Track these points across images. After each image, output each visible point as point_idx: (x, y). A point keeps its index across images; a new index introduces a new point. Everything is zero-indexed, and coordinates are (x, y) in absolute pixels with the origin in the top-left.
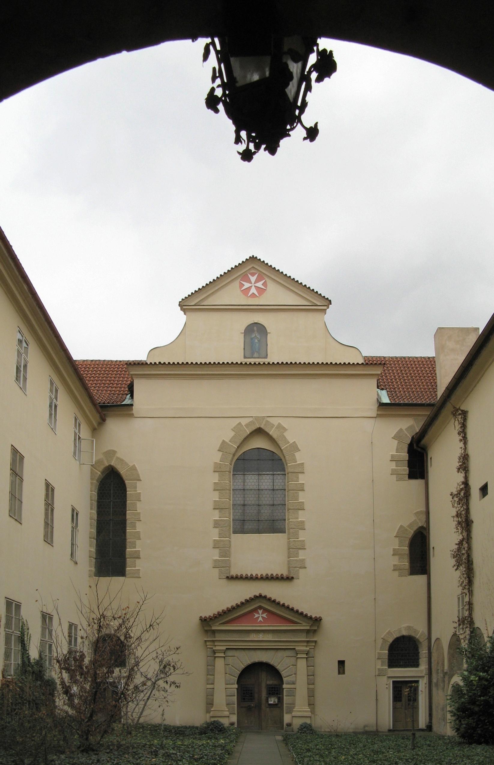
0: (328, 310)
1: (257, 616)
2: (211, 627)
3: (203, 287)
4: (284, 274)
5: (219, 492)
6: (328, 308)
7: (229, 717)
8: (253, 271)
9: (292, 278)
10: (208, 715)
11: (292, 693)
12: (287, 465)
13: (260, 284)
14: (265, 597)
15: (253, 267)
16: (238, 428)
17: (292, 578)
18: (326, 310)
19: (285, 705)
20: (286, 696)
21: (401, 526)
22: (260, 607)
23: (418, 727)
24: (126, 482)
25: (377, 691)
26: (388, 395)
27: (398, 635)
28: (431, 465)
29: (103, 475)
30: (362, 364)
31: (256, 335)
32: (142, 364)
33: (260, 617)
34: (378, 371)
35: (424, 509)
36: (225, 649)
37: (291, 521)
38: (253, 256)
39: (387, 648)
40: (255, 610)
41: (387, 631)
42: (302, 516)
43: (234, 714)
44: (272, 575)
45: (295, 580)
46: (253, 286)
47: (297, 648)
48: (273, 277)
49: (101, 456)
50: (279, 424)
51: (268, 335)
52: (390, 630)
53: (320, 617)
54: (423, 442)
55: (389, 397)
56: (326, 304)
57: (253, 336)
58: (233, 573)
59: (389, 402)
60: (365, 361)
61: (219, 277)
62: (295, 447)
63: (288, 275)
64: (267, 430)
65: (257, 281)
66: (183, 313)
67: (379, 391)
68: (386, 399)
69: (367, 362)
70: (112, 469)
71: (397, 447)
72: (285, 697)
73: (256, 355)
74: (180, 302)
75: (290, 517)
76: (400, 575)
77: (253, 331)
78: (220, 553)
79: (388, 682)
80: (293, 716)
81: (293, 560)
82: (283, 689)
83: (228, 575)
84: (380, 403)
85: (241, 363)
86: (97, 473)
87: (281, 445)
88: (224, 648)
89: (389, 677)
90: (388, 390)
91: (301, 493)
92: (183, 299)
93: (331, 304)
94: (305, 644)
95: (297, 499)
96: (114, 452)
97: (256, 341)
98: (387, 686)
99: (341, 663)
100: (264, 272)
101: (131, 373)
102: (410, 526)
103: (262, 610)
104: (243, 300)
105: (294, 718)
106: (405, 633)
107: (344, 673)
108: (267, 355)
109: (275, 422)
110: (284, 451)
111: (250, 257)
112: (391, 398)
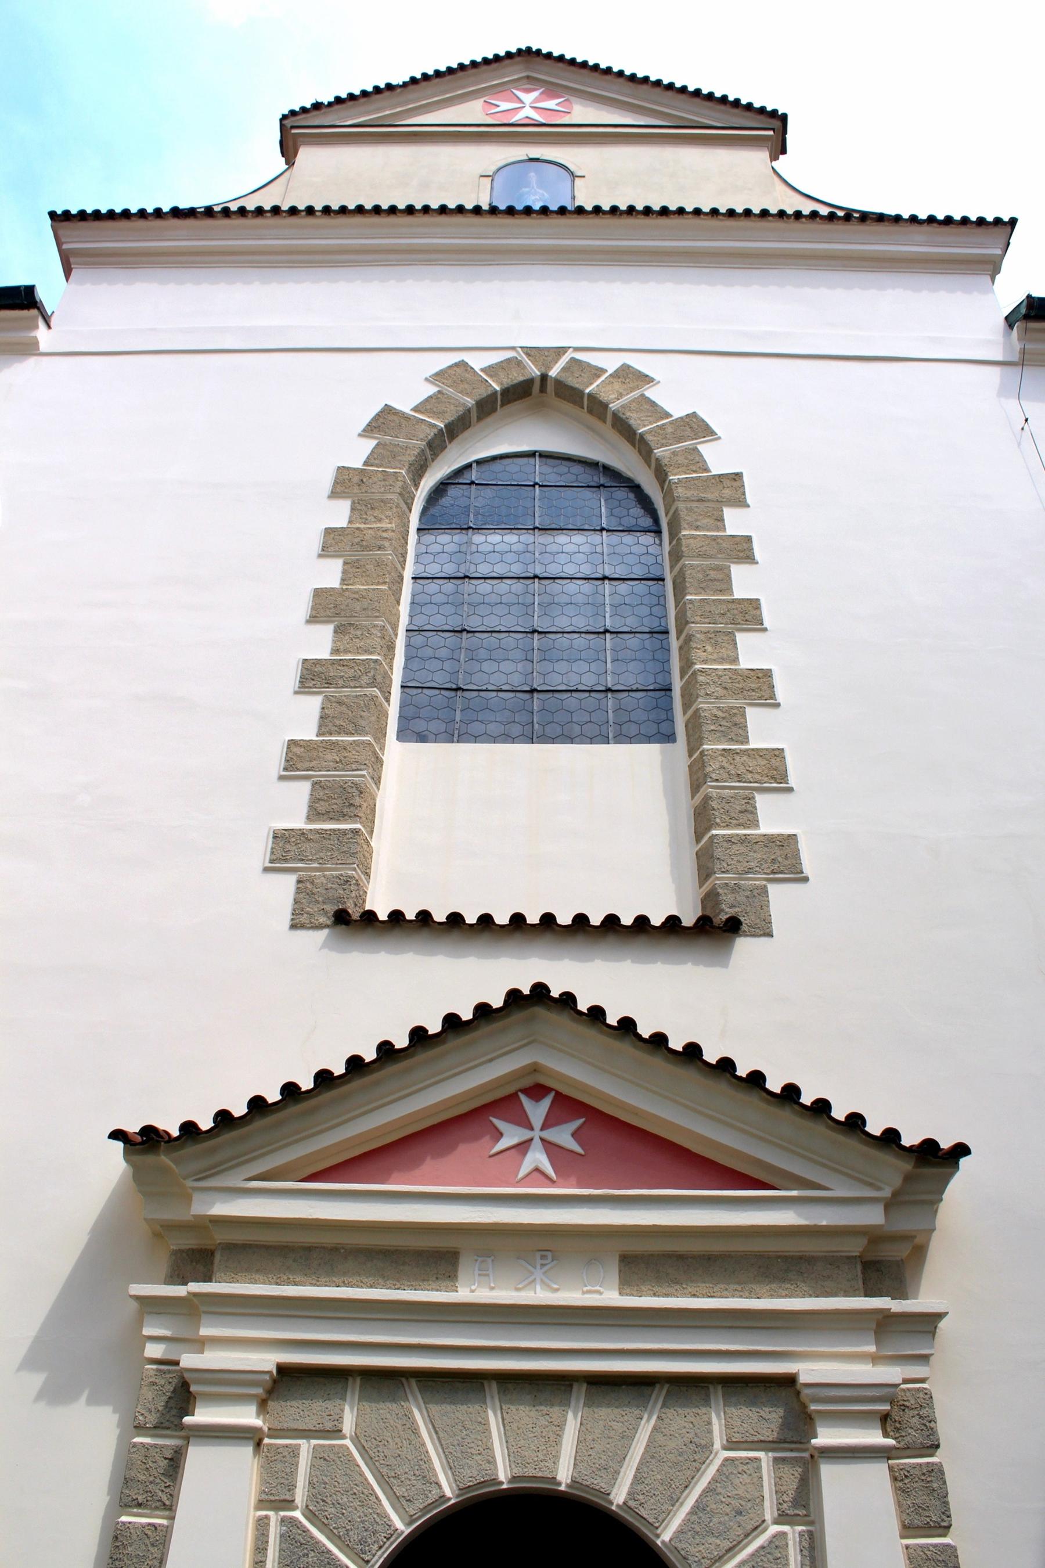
1: (512, 1135)
2: (188, 1199)
5: (345, 563)
17: (733, 927)
22: (537, 1091)
33: (537, 1143)
37: (702, 671)
81: (729, 840)
88: (267, 1361)
103: (546, 1103)
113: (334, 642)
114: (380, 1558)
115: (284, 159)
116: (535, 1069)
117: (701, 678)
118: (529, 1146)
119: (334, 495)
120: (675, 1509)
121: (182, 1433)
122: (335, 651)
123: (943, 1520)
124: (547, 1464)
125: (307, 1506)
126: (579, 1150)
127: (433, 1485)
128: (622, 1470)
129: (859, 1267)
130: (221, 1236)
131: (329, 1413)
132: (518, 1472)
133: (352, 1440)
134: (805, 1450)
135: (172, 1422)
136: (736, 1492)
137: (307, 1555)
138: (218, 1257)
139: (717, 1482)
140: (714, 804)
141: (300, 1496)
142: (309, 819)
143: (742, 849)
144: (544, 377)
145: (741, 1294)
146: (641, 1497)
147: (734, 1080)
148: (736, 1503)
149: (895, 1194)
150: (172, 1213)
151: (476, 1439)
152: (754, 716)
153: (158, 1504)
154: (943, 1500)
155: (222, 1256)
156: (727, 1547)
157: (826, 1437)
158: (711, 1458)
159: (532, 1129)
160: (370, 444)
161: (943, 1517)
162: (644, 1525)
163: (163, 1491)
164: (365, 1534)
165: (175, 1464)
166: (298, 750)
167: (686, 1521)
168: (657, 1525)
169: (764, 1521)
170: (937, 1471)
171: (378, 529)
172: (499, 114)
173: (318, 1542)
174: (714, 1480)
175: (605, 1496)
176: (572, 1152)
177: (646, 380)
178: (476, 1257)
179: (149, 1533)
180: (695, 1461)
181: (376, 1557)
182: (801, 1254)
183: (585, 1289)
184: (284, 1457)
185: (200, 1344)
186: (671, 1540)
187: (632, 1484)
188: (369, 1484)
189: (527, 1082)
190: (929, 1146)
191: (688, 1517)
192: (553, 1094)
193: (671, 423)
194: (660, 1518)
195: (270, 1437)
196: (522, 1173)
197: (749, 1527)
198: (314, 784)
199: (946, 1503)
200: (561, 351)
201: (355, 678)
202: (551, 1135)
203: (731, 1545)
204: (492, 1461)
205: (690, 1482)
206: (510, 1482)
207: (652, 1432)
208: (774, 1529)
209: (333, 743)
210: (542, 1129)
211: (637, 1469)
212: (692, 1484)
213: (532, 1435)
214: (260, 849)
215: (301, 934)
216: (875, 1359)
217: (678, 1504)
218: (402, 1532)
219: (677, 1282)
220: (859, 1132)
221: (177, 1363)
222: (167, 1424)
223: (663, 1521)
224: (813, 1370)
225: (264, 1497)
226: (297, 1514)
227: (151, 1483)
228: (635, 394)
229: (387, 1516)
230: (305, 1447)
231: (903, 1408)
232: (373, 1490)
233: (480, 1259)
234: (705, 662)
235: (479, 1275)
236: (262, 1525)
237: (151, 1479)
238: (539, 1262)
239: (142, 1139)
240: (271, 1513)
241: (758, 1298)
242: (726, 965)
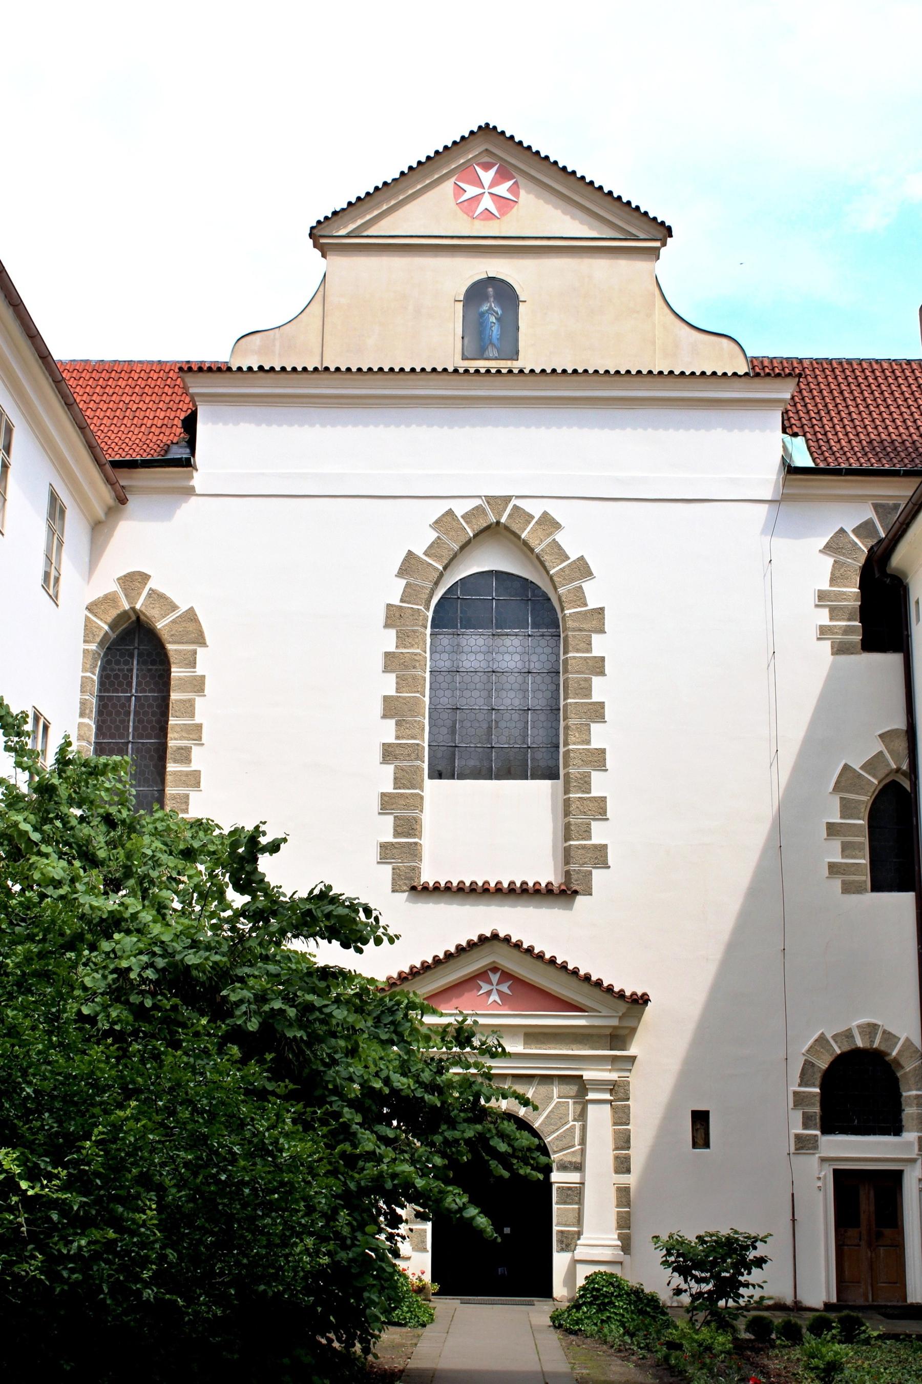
0: (663, 251)
1: (485, 988)
3: (368, 194)
4: (561, 165)
5: (397, 677)
6: (664, 244)
8: (486, 159)
9: (579, 175)
11: (575, 1194)
12: (563, 610)
13: (503, 189)
14: (507, 939)
15: (487, 150)
16: (446, 521)
17: (576, 892)
18: (658, 249)
19: (555, 1229)
20: (557, 1203)
21: (846, 767)
22: (495, 969)
23: (905, 1298)
24: (169, 647)
25: (793, 1195)
26: (809, 448)
27: (846, 1048)
28: (918, 620)
29: (114, 632)
30: (746, 374)
31: (491, 307)
32: (219, 370)
33: (495, 991)
34: (785, 391)
35: (900, 724)
38: (487, 125)
39: (818, 1082)
40: (482, 975)
41: (816, 1036)
42: (599, 736)
43: (424, 1250)
44: (524, 883)
45: (579, 899)
46: (487, 195)
47: (588, 1075)
48: (533, 173)
49: (113, 587)
50: (545, 514)
51: (522, 307)
52: (822, 1033)
53: (645, 994)
54: (898, 560)
55: (811, 454)
56: (660, 236)
57: (485, 308)
58: (428, 877)
59: (812, 465)
60: (753, 368)
61: (406, 171)
62: (582, 569)
63: (569, 170)
64: (515, 527)
65: (493, 184)
66: (320, 254)
67: (787, 438)
68: (803, 459)
69: (757, 370)
70: (138, 618)
71: (832, 574)
73: (492, 352)
74: (312, 228)
75: (571, 739)
76: (847, 888)
77: (486, 298)
78: (396, 827)
79: (823, 1173)
80: (577, 1258)
81: (577, 847)
83: (415, 884)
84: (789, 466)
85: (456, 371)
86: (100, 628)
87: (547, 564)
89: (823, 1160)
90: (809, 436)
91: (596, 681)
92: (319, 222)
93: (671, 236)
95: (589, 695)
96: (144, 577)
97: (493, 319)
98: (820, 1184)
99: (700, 1119)
100: (513, 161)
101: (191, 391)
102: (869, 766)
103: (498, 975)
104: (463, 226)
106: (860, 1043)
107: (707, 1145)
108: (517, 353)
109: (535, 509)
110: (556, 579)
111: (480, 127)
112: (815, 455)
113: (396, 731)
115: (311, 241)
116: (494, 962)
117: (572, 755)
119: (387, 626)
122: (397, 738)
140: (572, 828)
142: (395, 836)
143: (583, 852)
144: (498, 523)
152: (596, 776)
157: (591, 1096)
160: (402, 583)
166: (386, 799)
167: (544, 1121)
170: (629, 1106)
171: (413, 653)
172: (466, 203)
177: (557, 526)
193: (569, 565)
198: (395, 817)
200: (507, 499)
201: (409, 755)
202: (500, 988)
209: (402, 794)
214: (374, 853)
215: (396, 894)
216: (610, 1070)
219: (543, 1043)
228: (549, 540)
234: (574, 744)
242: (571, 909)
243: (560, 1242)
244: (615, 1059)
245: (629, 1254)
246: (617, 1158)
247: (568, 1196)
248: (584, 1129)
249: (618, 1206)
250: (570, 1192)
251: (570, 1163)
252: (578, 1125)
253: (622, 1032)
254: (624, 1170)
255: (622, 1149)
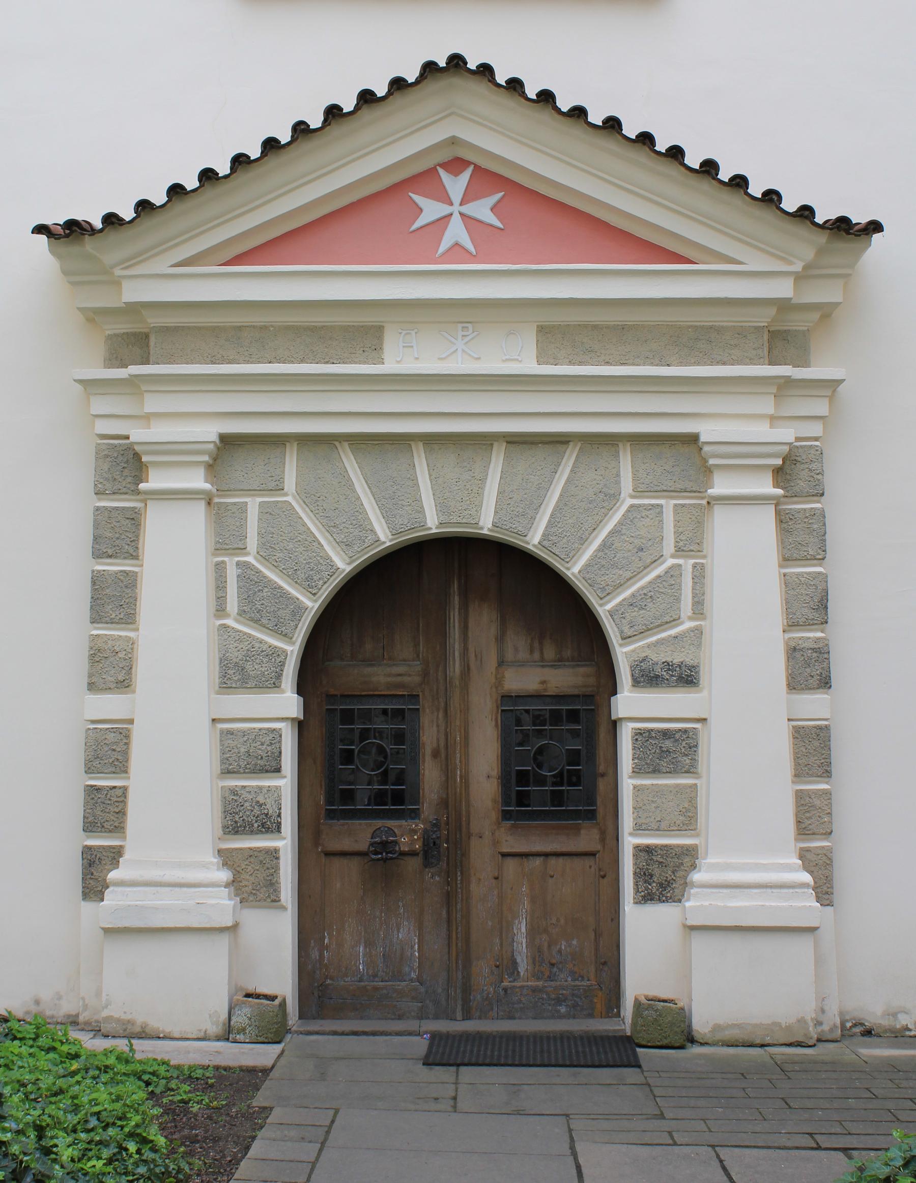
1: (431, 210)
2: (117, 283)
7: (234, 928)
10: (88, 908)
19: (629, 841)
20: (637, 771)
22: (456, 165)
33: (456, 218)
36: (214, 438)
47: (708, 431)
72: (628, 784)
82: (614, 725)
94: (767, 406)
103: (466, 175)
105: (699, 942)
114: (325, 591)
118: (448, 223)
120: (584, 547)
121: (139, 497)
123: (819, 554)
124: (470, 512)
125: (258, 553)
126: (501, 226)
127: (369, 532)
128: (538, 516)
129: (766, 337)
130: (154, 320)
131: (270, 475)
132: (444, 519)
133: (294, 497)
134: (703, 498)
135: (129, 489)
136: (639, 533)
137: (262, 590)
138: (152, 340)
139: (622, 525)
141: (252, 542)
145: (652, 361)
146: (554, 538)
147: (653, 154)
148: (637, 542)
149: (806, 268)
150: (101, 299)
151: (406, 492)
153: (126, 555)
154: (820, 538)
155: (156, 339)
156: (628, 577)
157: (721, 486)
158: (617, 505)
159: (451, 204)
161: (820, 551)
162: (555, 560)
163: (128, 545)
164: (311, 573)
165: (135, 520)
167: (594, 556)
168: (568, 560)
169: (662, 556)
173: (270, 581)
174: (620, 523)
175: (522, 538)
176: (491, 225)
178: (400, 331)
179: (122, 578)
180: (603, 507)
181: (322, 591)
182: (711, 324)
183: (504, 358)
184: (233, 513)
185: (147, 418)
186: (580, 572)
187: (546, 527)
188: (311, 532)
189: (445, 155)
190: (842, 225)
191: (595, 554)
192: (471, 168)
194: (571, 555)
195: (219, 496)
196: (442, 248)
197: (649, 561)
199: (825, 541)
202: (468, 209)
203: (631, 575)
204: (421, 511)
205: (598, 525)
206: (437, 528)
207: (565, 484)
208: (671, 562)
210: (461, 204)
211: (551, 515)
212: (600, 527)
213: (457, 488)
216: (774, 420)
217: (586, 543)
218: (344, 570)
220: (775, 208)
221: (127, 438)
222: (124, 490)
223: (573, 557)
224: (714, 430)
225: (218, 546)
226: (250, 559)
227: (118, 538)
229: (329, 558)
230: (253, 504)
231: (794, 462)
232: (315, 537)
233: (404, 332)
235: (404, 347)
236: (220, 568)
237: (117, 535)
238: (460, 333)
239: (64, 232)
240: (226, 559)
241: (668, 365)
243: (643, 875)
244: (785, 386)
245: (830, 904)
246: (793, 651)
247: (664, 753)
248: (700, 573)
249: (798, 775)
250: (668, 744)
251: (669, 666)
252: (688, 564)
253: (797, 322)
254: (814, 682)
255: (808, 624)
